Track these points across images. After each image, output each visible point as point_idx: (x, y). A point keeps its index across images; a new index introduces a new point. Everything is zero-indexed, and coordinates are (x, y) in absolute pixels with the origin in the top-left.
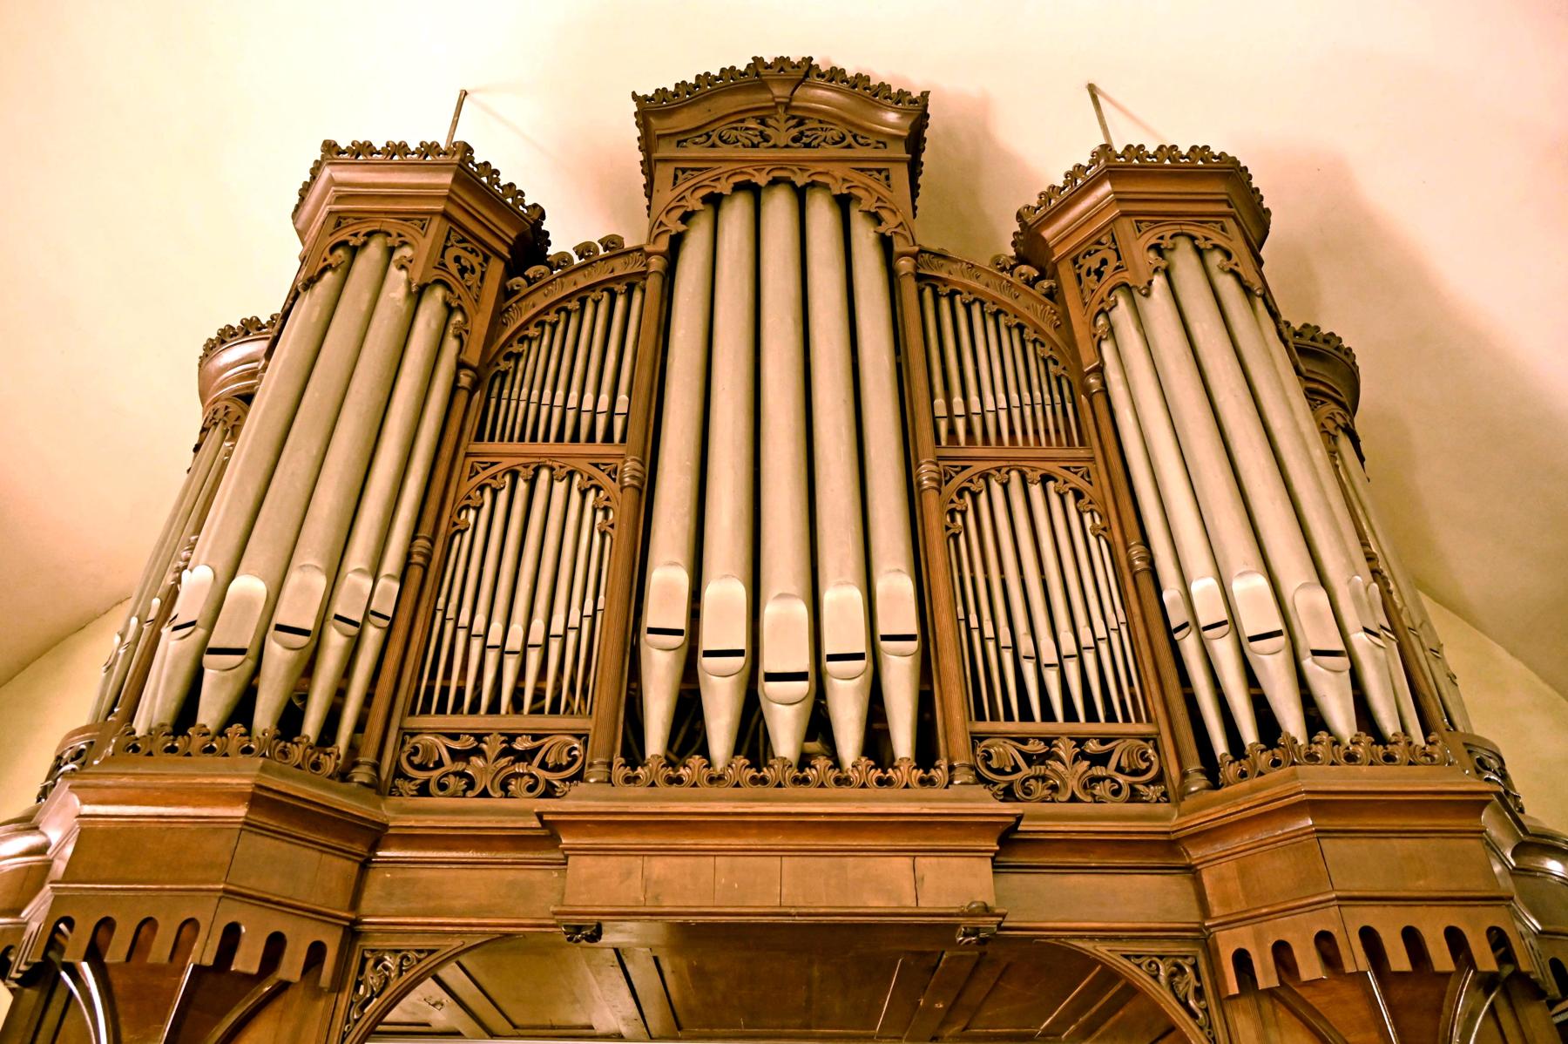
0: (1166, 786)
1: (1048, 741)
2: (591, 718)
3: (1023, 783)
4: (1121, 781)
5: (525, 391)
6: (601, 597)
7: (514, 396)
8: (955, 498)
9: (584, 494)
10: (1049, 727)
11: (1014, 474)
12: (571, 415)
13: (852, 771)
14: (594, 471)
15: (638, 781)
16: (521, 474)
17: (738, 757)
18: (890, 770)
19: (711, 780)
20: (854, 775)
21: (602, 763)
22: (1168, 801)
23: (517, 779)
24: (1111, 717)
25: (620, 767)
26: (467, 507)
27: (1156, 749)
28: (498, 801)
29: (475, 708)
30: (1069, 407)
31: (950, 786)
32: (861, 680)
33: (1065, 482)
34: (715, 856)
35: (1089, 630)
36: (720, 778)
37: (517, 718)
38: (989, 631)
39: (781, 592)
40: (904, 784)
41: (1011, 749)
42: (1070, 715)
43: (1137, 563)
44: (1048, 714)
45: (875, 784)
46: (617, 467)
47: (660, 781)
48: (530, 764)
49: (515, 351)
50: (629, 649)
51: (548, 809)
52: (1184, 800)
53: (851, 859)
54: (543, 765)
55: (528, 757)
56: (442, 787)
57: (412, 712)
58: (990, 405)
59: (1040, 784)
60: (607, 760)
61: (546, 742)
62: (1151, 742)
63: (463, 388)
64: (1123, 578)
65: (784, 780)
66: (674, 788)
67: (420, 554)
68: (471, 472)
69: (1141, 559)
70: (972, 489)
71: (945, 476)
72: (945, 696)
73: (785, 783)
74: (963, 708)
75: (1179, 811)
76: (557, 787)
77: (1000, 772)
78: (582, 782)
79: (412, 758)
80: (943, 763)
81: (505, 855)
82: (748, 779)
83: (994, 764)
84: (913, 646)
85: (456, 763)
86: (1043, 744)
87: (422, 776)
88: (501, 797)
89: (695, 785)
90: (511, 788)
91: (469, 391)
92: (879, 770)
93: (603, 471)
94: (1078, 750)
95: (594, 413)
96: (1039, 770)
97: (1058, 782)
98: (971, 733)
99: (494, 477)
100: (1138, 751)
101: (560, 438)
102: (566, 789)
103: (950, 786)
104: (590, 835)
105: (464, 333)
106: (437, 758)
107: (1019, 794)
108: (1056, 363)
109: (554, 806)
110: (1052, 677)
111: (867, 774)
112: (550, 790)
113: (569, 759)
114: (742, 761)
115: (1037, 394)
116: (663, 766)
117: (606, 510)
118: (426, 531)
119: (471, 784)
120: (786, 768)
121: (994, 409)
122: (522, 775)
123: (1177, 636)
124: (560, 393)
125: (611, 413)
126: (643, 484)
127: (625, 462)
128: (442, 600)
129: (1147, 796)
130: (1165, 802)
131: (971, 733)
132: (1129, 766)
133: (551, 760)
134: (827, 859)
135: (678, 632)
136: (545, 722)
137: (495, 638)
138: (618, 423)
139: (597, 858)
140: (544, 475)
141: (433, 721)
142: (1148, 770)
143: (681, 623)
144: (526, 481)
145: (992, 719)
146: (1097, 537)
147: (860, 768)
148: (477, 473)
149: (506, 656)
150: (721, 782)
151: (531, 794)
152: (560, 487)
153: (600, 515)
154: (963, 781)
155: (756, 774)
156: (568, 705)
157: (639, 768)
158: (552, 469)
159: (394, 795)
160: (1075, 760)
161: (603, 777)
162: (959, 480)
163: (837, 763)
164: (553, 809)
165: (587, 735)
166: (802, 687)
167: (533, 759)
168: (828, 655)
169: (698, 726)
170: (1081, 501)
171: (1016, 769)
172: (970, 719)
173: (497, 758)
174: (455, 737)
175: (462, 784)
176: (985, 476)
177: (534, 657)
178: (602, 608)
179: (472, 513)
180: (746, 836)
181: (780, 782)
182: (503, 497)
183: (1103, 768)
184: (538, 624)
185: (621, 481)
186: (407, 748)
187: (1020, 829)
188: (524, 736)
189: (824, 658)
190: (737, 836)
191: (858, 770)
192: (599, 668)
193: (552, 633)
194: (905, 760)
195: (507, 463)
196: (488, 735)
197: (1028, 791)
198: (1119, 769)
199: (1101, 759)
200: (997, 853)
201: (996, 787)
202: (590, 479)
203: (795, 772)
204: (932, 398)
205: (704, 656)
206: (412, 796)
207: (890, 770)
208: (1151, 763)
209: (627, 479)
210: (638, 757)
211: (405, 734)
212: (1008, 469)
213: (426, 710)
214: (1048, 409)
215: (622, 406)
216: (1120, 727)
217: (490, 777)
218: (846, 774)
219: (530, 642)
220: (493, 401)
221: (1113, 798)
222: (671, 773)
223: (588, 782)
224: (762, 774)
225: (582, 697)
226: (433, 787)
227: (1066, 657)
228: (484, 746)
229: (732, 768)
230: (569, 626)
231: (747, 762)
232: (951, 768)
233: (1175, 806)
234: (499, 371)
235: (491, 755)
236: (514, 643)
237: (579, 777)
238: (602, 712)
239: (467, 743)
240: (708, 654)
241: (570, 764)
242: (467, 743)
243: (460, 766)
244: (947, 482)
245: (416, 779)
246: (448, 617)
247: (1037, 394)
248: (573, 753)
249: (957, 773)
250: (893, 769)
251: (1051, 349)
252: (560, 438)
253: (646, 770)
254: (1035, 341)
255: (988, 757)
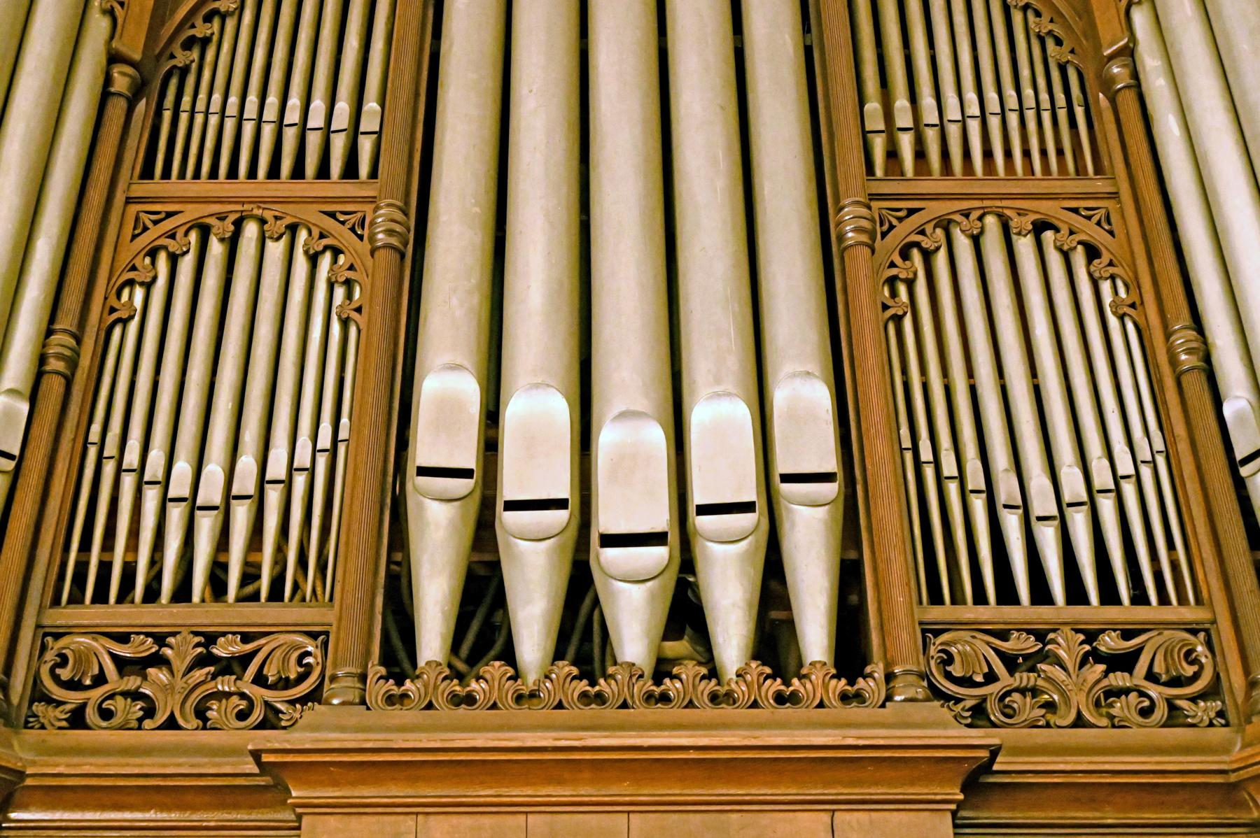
0: (1223, 702)
1: (1040, 636)
2: (333, 606)
3: (1002, 699)
4: (1153, 694)
5: (217, 98)
6: (345, 420)
7: (200, 106)
8: (897, 260)
9: (313, 260)
10: (1043, 613)
11: (990, 220)
12: (290, 135)
13: (737, 683)
14: (329, 223)
15: (406, 701)
16: (214, 230)
17: (560, 663)
18: (795, 681)
19: (519, 698)
20: (740, 689)
21: (349, 675)
22: (1227, 725)
23: (220, 701)
24: (1140, 598)
25: (378, 680)
26: (131, 283)
27: (1209, 644)
28: (190, 735)
29: (152, 594)
30: (1079, 112)
31: (888, 704)
32: (750, 543)
33: (1072, 233)
34: (526, 813)
35: (1106, 463)
36: (533, 695)
37: (217, 607)
38: (949, 468)
39: (624, 409)
40: (817, 702)
41: (983, 647)
42: (1076, 594)
43: (1183, 357)
44: (1041, 593)
45: (772, 701)
46: (364, 219)
47: (440, 702)
48: (239, 678)
49: (199, 35)
50: (388, 501)
51: (269, 746)
52: (1250, 722)
53: (734, 816)
54: (260, 680)
55: (237, 668)
57: (56, 601)
58: (953, 112)
59: (1028, 699)
60: (359, 671)
61: (263, 645)
62: (1202, 635)
63: (120, 95)
64: (1160, 381)
65: (632, 697)
67: (59, 357)
68: (135, 228)
69: (1189, 351)
70: (924, 245)
71: (882, 225)
72: (881, 566)
73: (634, 702)
74: (908, 584)
75: (1243, 739)
76: (283, 713)
77: (966, 682)
78: (320, 703)
79: (58, 671)
80: (877, 669)
81: (205, 816)
82: (576, 695)
83: (957, 670)
84: (830, 490)
85: (126, 678)
86: (1032, 638)
87: (75, 698)
88: (196, 729)
89: (494, 706)
90: (209, 714)
91: (127, 98)
92: (779, 681)
93: (343, 223)
94: (1087, 648)
95: (327, 131)
96: (1023, 678)
97: (1056, 697)
98: (921, 623)
100: (1180, 650)
101: (274, 172)
102: (297, 715)
103: (888, 704)
104: (335, 784)
105: (117, 8)
106: (96, 671)
107: (995, 716)
108: (1059, 42)
109: (278, 742)
110: (1048, 537)
111: (759, 687)
112: (271, 716)
113: (301, 670)
114: (566, 668)
115: (1028, 92)
116: (445, 678)
117: (348, 283)
118: (66, 321)
119: (150, 712)
120: (634, 679)
121: (959, 118)
122: (228, 695)
123: (1244, 471)
124: (273, 100)
125: (355, 132)
126: (406, 244)
127: (375, 210)
128: (96, 428)
129: (1194, 717)
130: (1223, 726)
131: (921, 623)
132: (1168, 671)
133: (271, 673)
134: (698, 816)
135: (465, 473)
136: (262, 613)
137: (180, 485)
138: (366, 146)
139: (346, 818)
140: (251, 230)
141: (89, 614)
142: (1196, 677)
143: (468, 458)
144: (222, 240)
145: (954, 602)
146: (1121, 318)
147: (748, 677)
148: (145, 229)
149: (198, 513)
150: (535, 701)
152: (276, 250)
153: (340, 292)
154: (907, 696)
155: (588, 688)
156: (296, 587)
157: (408, 682)
158: (262, 221)
159: (32, 728)
160: (1083, 663)
161: (354, 696)
162: (904, 231)
163: (714, 673)
164: (277, 746)
165: (327, 633)
166: (657, 555)
167: (245, 668)
168: (698, 506)
169: (498, 617)
170: (1096, 262)
171: (991, 677)
172: (921, 602)
173: (190, 669)
174: (123, 638)
176: (946, 225)
177: (241, 515)
179: (139, 293)
180: (574, 782)
181: (625, 700)
182: (186, 266)
183: (1126, 675)
184: (247, 463)
185: (372, 239)
186: (50, 656)
187: (995, 767)
188: (230, 636)
189: (692, 510)
190: (560, 782)
191: (745, 681)
192: (343, 529)
193: (268, 477)
194: (818, 666)
195: (192, 212)
196: (174, 634)
197: (1009, 712)
198: (1151, 677)
199: (1124, 662)
200: (960, 805)
201: (961, 706)
202: (322, 236)
203: (649, 686)
204: (862, 103)
205: (505, 509)
206: (60, 728)
207: (795, 681)
208: (1202, 667)
209: (380, 236)
210: (406, 665)
211: (46, 635)
212: (981, 212)
213: (77, 599)
214: (1046, 116)
215: (369, 122)
216: (1153, 612)
217: (179, 698)
218: (726, 688)
219: (235, 491)
220: (167, 115)
221: (1140, 720)
222: (458, 688)
223: (331, 704)
224: (597, 688)
225: (318, 575)
226: (91, 715)
227: (1070, 505)
228: (168, 652)
229: (552, 681)
230: (295, 466)
231: (575, 671)
232: (890, 677)
233: (1237, 732)
234: (175, 67)
235: (180, 666)
236: (211, 492)
237: (315, 696)
238: (349, 600)
239: (141, 647)
240: (512, 506)
241: (302, 678)
242: (142, 648)
243: (132, 682)
244: (884, 235)
245: (64, 703)
246: (106, 454)
247: (1028, 92)
248: (305, 661)
249: (898, 684)
250: (800, 679)
251: (1051, 21)
252: (274, 172)
253: (419, 684)
254: (1025, 8)
255: (949, 660)
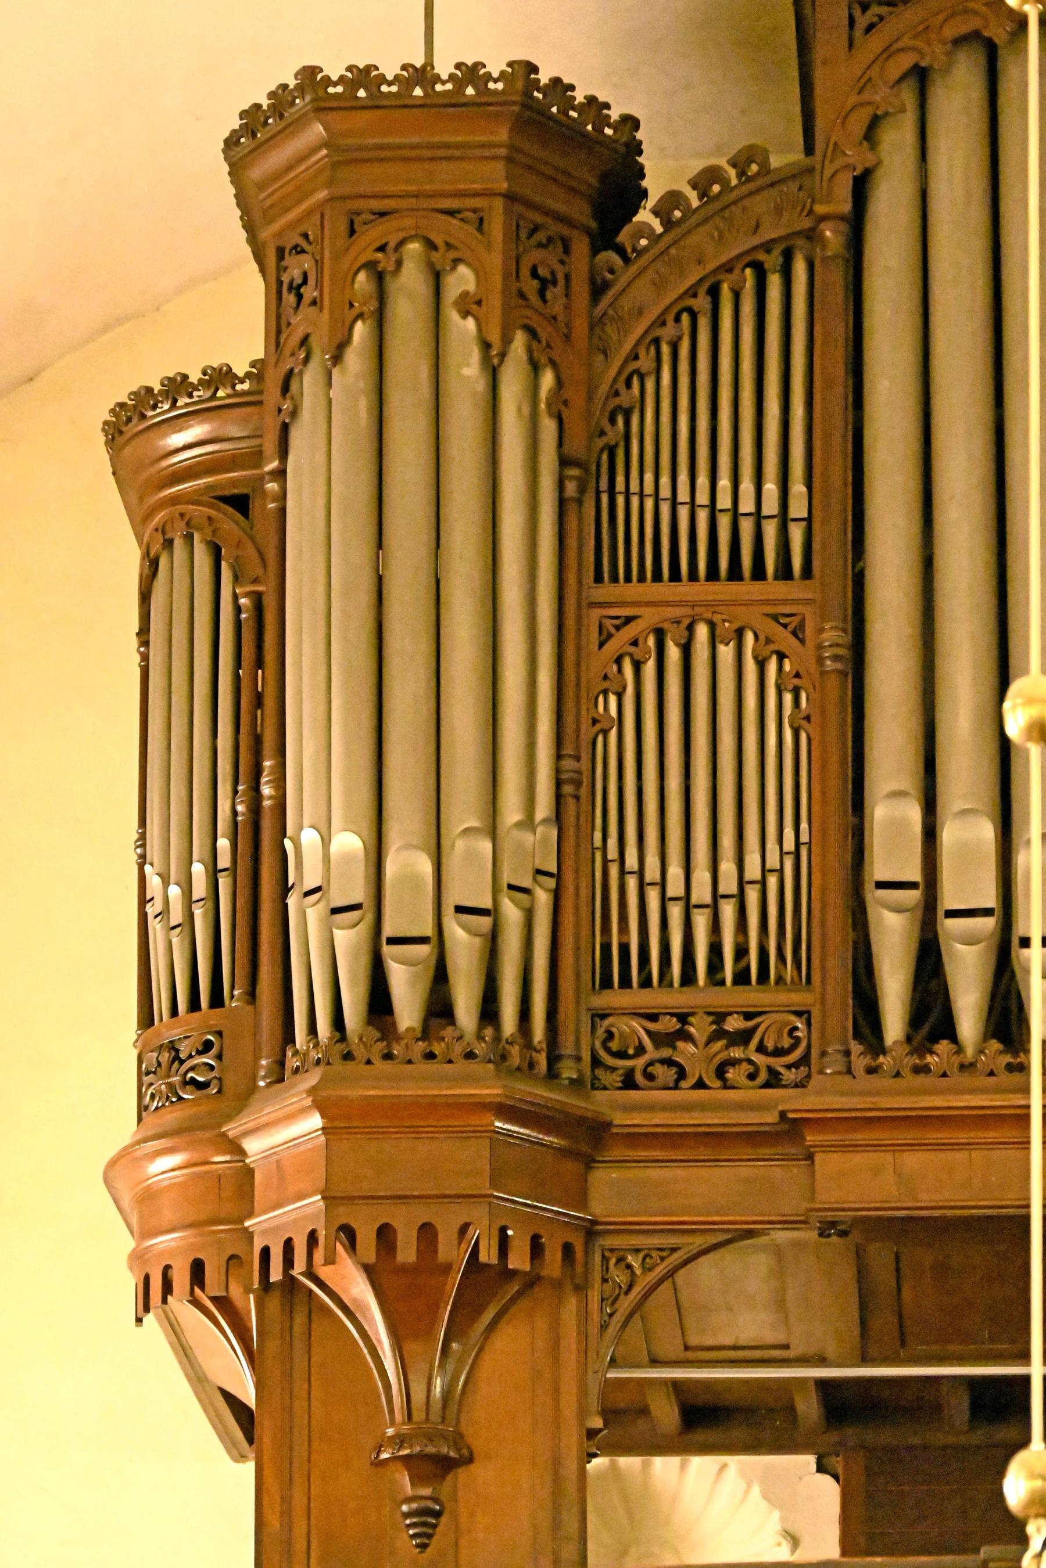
19: (962, 1067)
36: (972, 1065)
56: (650, 1077)
66: (921, 1079)
89: (944, 1075)
99: (635, 643)
113: (792, 1041)
114: (995, 1045)
119: (682, 1074)
133: (770, 1045)
151: (751, 1083)
165: (809, 1012)
175: (672, 1073)
178: (807, 840)
182: (649, 669)
196: (692, 1014)
222: (917, 1061)
226: (639, 1078)
243: (666, 1053)
